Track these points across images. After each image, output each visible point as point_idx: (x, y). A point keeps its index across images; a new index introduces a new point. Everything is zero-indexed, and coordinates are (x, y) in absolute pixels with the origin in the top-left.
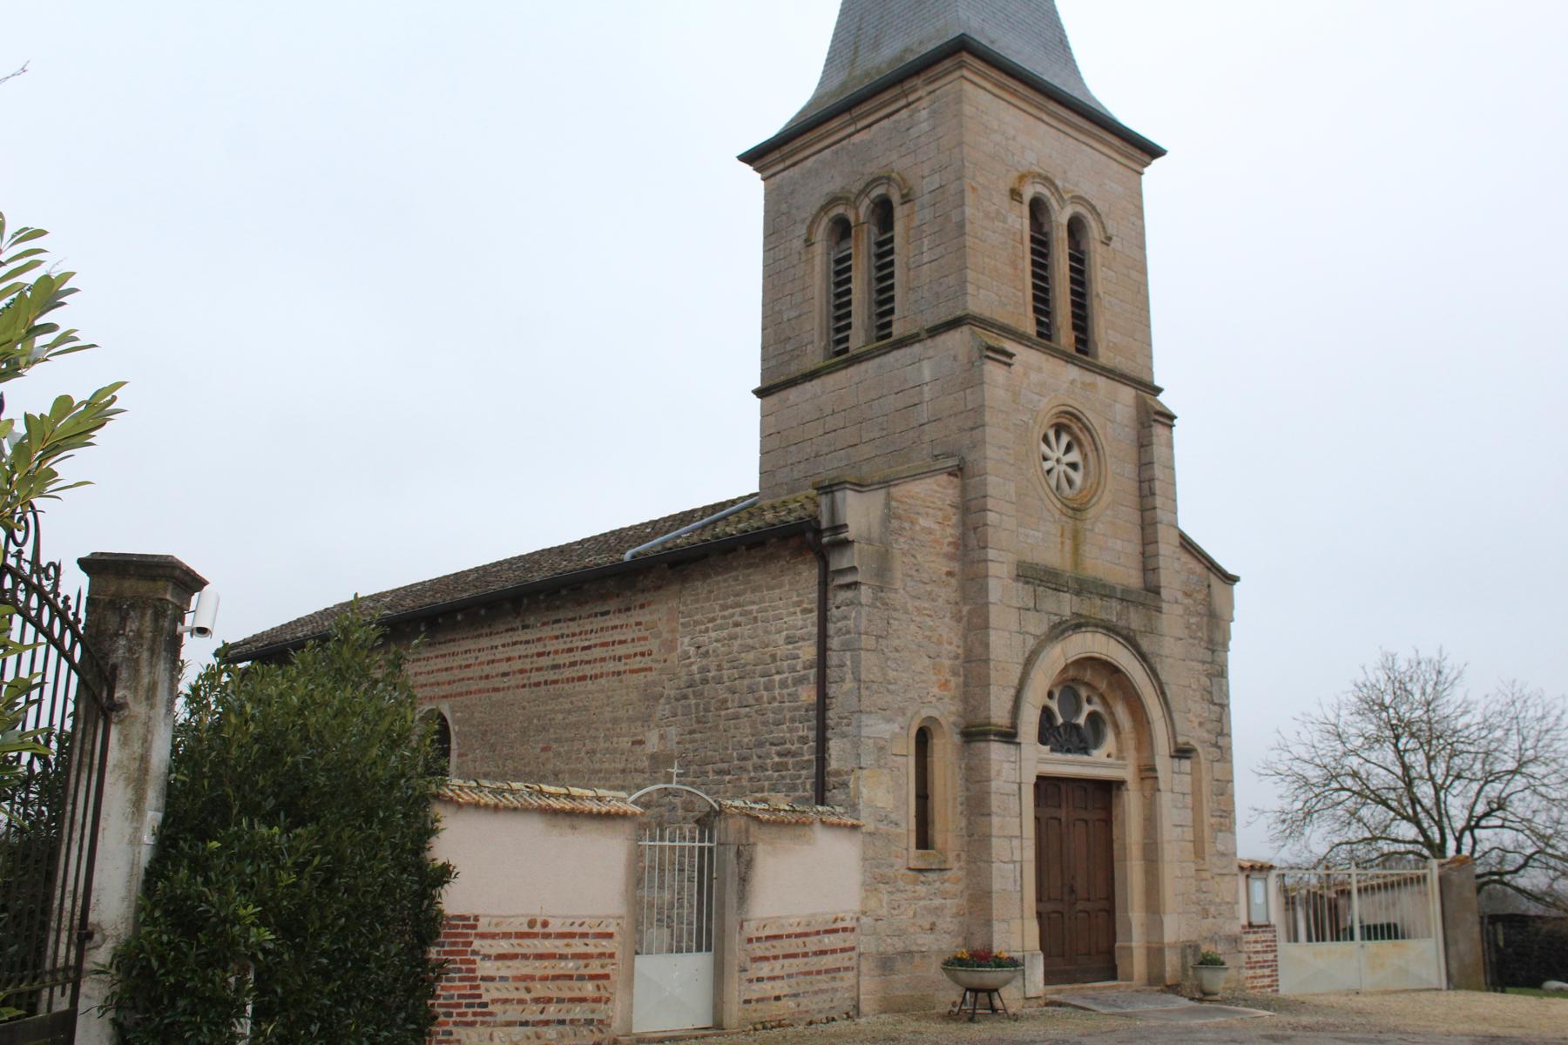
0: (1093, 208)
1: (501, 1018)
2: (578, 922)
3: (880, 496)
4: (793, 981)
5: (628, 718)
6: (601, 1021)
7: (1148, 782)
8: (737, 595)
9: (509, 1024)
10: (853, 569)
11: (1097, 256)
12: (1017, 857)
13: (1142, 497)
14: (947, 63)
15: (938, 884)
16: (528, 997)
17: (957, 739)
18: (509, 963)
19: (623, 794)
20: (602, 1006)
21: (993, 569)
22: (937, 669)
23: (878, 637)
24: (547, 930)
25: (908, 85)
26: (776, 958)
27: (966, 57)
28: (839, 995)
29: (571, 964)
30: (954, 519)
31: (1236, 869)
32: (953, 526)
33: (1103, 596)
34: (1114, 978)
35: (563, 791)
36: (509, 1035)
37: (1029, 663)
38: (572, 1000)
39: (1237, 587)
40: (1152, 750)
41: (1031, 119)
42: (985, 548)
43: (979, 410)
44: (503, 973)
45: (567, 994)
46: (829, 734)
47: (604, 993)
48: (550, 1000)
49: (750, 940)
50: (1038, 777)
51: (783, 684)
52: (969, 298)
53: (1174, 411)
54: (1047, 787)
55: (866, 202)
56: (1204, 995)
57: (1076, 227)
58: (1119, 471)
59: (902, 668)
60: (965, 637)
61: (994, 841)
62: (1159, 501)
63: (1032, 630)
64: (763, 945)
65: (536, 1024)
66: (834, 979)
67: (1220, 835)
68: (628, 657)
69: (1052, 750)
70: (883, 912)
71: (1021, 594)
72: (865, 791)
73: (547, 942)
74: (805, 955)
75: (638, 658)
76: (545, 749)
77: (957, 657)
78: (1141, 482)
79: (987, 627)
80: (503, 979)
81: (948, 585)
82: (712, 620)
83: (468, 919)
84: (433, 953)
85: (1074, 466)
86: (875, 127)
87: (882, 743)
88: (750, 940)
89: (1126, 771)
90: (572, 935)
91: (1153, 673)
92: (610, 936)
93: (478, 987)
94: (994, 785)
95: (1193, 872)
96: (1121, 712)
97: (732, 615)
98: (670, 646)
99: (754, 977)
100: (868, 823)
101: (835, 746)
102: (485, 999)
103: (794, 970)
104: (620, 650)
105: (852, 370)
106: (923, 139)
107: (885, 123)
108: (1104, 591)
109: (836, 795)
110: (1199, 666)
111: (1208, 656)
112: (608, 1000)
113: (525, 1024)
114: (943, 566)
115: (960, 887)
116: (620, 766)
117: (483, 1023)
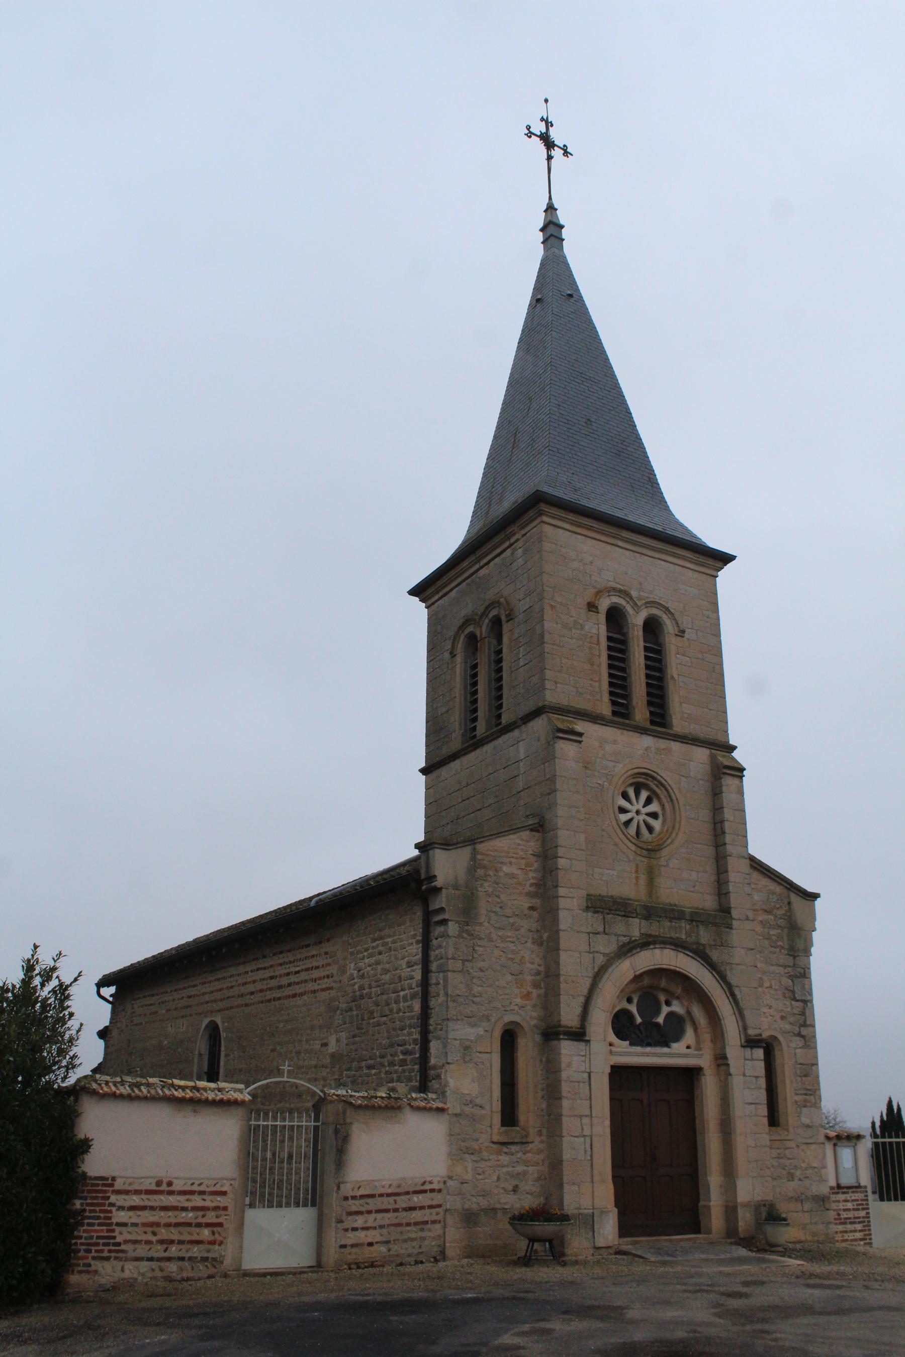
0: (667, 610)
1: (131, 1254)
2: (197, 1182)
3: (467, 851)
4: (384, 1231)
5: (320, 1026)
6: (214, 1259)
7: (723, 1068)
8: (380, 931)
9: (137, 1259)
10: (442, 910)
11: (671, 643)
12: (587, 1132)
13: (716, 836)
14: (531, 513)
15: (519, 1155)
16: (154, 1239)
17: (538, 1038)
18: (139, 1213)
19: (242, 1086)
20: (217, 1247)
21: (562, 903)
23: (464, 961)
24: (171, 1188)
25: (509, 530)
26: (369, 1212)
27: (543, 507)
28: (426, 1243)
29: (191, 1215)
30: (536, 865)
31: (822, 1138)
32: (535, 871)
33: (671, 919)
34: (698, 1231)
35: (191, 1084)
36: (137, 1267)
38: (192, 1242)
39: (818, 902)
40: (724, 1042)
41: (609, 547)
42: (557, 886)
43: (552, 780)
44: (134, 1220)
45: (187, 1237)
46: (430, 1036)
47: (217, 1236)
48: (172, 1242)
49: (346, 1198)
50: (612, 1067)
51: (405, 999)
52: (547, 692)
53: (745, 765)
54: (620, 1075)
55: (487, 621)
56: (770, 1247)
57: (652, 627)
58: (693, 817)
59: (488, 983)
60: (545, 957)
61: (564, 1118)
62: (728, 838)
63: (602, 950)
64: (357, 1202)
65: (159, 1259)
66: (422, 1230)
67: (804, 1110)
68: (320, 979)
70: (469, 1177)
71: (593, 921)
72: (452, 1082)
73: (171, 1198)
74: (396, 1210)
75: (326, 980)
76: (273, 1050)
77: (538, 973)
78: (715, 824)
79: (558, 949)
80: (135, 1225)
81: (530, 917)
82: (367, 950)
83: (107, 1179)
84: (78, 1204)
85: (654, 815)
86: (492, 564)
87: (468, 1043)
88: (346, 1198)
89: (704, 1060)
90: (192, 1193)
91: (722, 978)
92: (224, 1193)
93: (113, 1231)
94: (564, 1075)
95: (768, 1143)
97: (377, 946)
98: (343, 970)
99: (350, 1226)
100: (453, 1106)
101: (434, 1046)
102: (118, 1240)
103: (386, 1222)
104: (316, 974)
105: (478, 752)
106: (520, 571)
107: (497, 560)
108: (673, 914)
109: (434, 1084)
110: (781, 970)
111: (790, 961)
112: (221, 1243)
113: (151, 1259)
114: (526, 903)
115: (542, 1156)
116: (314, 1063)
117: (116, 1258)
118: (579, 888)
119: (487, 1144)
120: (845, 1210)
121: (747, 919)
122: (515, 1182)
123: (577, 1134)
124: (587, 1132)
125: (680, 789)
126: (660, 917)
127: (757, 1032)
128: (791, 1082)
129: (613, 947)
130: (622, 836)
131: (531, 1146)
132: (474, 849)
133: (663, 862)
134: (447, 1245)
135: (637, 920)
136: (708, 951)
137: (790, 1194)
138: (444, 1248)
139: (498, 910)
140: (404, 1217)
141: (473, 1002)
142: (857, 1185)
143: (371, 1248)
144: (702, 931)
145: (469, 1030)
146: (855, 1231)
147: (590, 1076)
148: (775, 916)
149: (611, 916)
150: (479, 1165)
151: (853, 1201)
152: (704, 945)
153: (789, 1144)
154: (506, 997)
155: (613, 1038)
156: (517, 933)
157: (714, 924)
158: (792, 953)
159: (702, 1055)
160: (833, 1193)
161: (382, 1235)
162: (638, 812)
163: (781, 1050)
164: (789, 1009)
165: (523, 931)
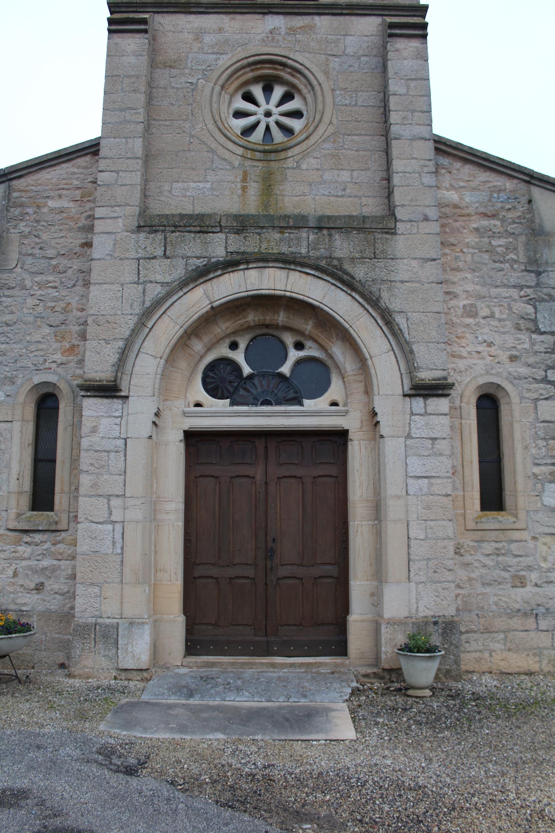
15: (46, 546)
22: (60, 337)
33: (282, 229)
37: (148, 313)
50: (185, 432)
63: (159, 278)
69: (232, 404)
71: (153, 244)
89: (352, 421)
96: (338, 351)
110: (514, 293)
111: (531, 279)
121: (426, 219)
122: (37, 579)
125: (326, 73)
126: (262, 228)
129: (179, 271)
130: (223, 140)
131: (63, 534)
132: (9, 186)
133: (290, 163)
135: (222, 236)
136: (347, 266)
137: (517, 606)
139: (37, 251)
144: (338, 239)
147: (126, 444)
148: (503, 220)
149: (177, 234)
152: (339, 260)
153: (516, 535)
155: (202, 395)
156: (62, 275)
157: (359, 230)
158: (534, 268)
159: (347, 412)
162: (268, 114)
163: (509, 403)
164: (526, 346)
165: (70, 272)
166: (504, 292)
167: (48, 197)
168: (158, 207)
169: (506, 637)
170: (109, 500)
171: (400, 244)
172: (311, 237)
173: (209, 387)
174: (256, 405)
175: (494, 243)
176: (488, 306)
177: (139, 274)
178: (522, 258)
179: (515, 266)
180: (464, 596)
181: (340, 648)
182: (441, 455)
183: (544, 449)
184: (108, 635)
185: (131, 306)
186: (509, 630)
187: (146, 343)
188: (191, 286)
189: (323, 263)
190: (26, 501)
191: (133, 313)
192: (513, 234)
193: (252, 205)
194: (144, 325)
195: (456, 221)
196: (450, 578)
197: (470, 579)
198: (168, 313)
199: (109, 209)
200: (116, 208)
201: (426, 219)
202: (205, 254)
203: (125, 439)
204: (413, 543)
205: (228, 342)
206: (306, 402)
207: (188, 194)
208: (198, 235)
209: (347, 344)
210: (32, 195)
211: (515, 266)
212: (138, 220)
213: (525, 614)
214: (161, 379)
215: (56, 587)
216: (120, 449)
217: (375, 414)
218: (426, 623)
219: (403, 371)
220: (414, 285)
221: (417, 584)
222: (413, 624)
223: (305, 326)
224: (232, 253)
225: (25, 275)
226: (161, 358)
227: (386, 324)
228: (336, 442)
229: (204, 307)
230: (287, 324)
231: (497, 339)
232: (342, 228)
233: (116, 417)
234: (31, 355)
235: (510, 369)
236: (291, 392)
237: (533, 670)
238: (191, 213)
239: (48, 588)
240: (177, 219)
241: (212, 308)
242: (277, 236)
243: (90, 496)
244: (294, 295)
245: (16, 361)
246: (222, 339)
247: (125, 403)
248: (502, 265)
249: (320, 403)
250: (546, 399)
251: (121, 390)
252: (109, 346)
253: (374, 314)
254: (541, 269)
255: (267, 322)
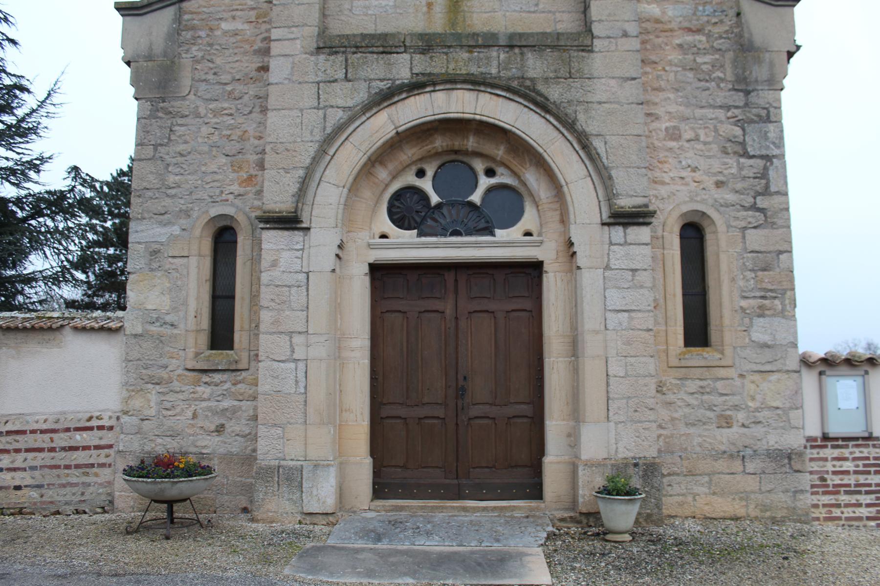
4: (37, 473)
12: (299, 354)
22: (237, 167)
23: (156, 147)
26: (17, 451)
28: (91, 489)
33: (471, 48)
50: (370, 265)
63: (340, 102)
67: (759, 322)
69: (420, 235)
70: (152, 412)
71: (333, 66)
74: (52, 450)
87: (155, 246)
89: (546, 252)
96: (532, 178)
110: (721, 114)
118: (305, 25)
119: (180, 372)
120: (835, 473)
121: (625, 35)
122: (218, 421)
123: (283, 358)
124: (299, 354)
126: (450, 47)
127: (640, 201)
128: (733, 280)
129: (361, 95)
131: (244, 374)
132: (180, 8)
134: (117, 494)
135: (406, 56)
136: (540, 87)
137: (723, 448)
138: (113, 497)
139: (210, 77)
140: (61, 458)
141: (168, 196)
142: (866, 435)
143: (19, 493)
144: (531, 58)
145: (159, 230)
146: (859, 505)
147: (308, 278)
148: (709, 35)
149: (359, 55)
150: (167, 398)
151: (855, 459)
152: (532, 80)
153: (722, 373)
154: (216, 184)
156: (237, 102)
157: (554, 47)
158: (743, 87)
159: (542, 242)
160: (813, 447)
161: (33, 478)
163: (715, 232)
164: (734, 171)
165: (246, 97)
166: (709, 113)
167: (221, 19)
168: (337, 27)
169: (711, 480)
170: (291, 337)
171: (597, 63)
172: (502, 56)
173: (395, 217)
174: (445, 236)
175: (699, 60)
176: (692, 129)
177: (319, 98)
178: (730, 76)
179: (722, 85)
180: (667, 437)
181: (536, 492)
182: (641, 287)
183: (752, 282)
184: (291, 478)
185: (311, 132)
186: (714, 473)
187: (327, 172)
188: (375, 110)
189: (515, 84)
190: (204, 339)
191: (314, 139)
192: (720, 50)
193: (438, 24)
194: (325, 152)
195: (658, 37)
196: (652, 418)
197: (673, 419)
198: (351, 139)
199: (286, 30)
200: (293, 29)
201: (625, 35)
202: (389, 76)
203: (307, 273)
204: (612, 380)
205: (414, 169)
206: (498, 232)
207: (370, 12)
208: (381, 56)
209: (542, 171)
210: (204, 17)
211: (722, 85)
212: (317, 41)
213: (731, 456)
214: (344, 209)
215: (237, 429)
216: (302, 284)
217: (571, 244)
218: (626, 465)
219: (601, 199)
220: (613, 106)
221: (616, 423)
222: (612, 465)
223: (496, 152)
224: (417, 74)
225: (199, 103)
226: (344, 187)
227: (583, 148)
228: (530, 274)
229: (389, 132)
230: (477, 150)
231: (702, 164)
232: (534, 46)
233: (298, 250)
234: (207, 186)
235: (716, 196)
236: (482, 222)
237: (739, 515)
238: (373, 32)
239: (228, 430)
240: (359, 39)
241: (397, 133)
242: (466, 55)
243: (271, 333)
244: (484, 118)
245: (191, 193)
246: (408, 166)
247: (306, 235)
248: (708, 84)
249: (514, 233)
250: (755, 227)
251: (302, 221)
252: (289, 175)
253: (569, 137)
254: (750, 88)
255: (456, 148)
